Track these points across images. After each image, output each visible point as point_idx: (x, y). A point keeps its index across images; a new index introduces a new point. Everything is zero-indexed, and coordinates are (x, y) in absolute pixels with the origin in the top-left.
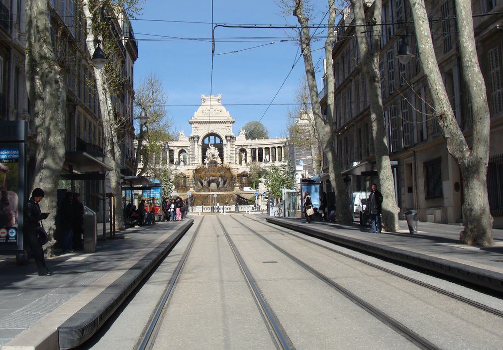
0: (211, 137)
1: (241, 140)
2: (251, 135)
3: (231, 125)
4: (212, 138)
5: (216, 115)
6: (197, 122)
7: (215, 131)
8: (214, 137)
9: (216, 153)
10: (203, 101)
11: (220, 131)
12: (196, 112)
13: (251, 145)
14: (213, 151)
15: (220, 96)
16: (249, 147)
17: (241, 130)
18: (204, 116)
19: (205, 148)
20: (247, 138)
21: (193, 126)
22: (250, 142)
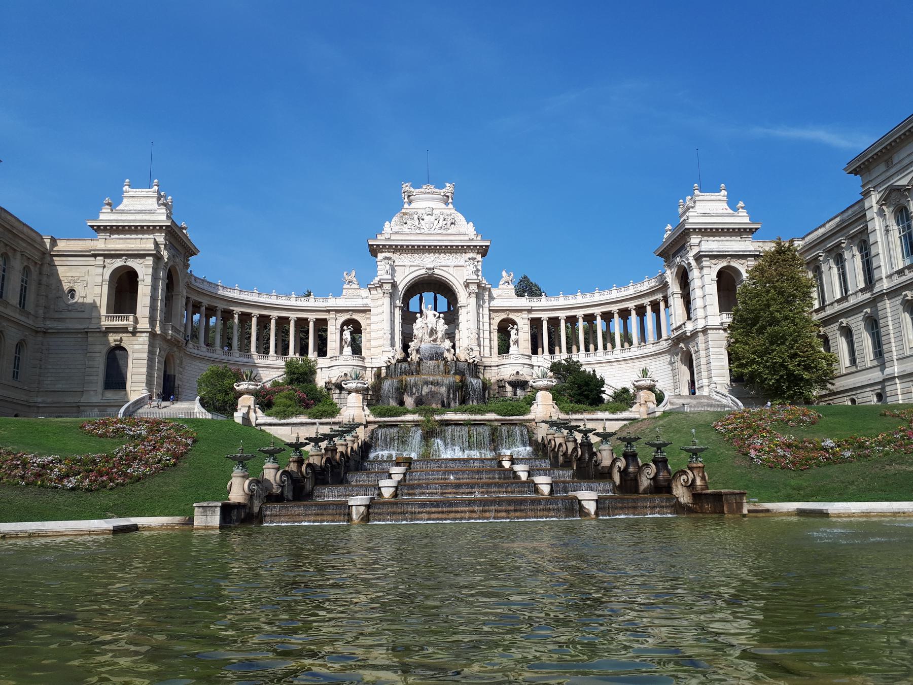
0: (424, 294)
1: (505, 296)
2: (526, 288)
3: (479, 257)
4: (428, 296)
5: (440, 232)
6: (390, 246)
7: (437, 271)
8: (432, 294)
9: (442, 327)
10: (406, 200)
11: (451, 270)
12: (387, 222)
13: (530, 311)
14: (429, 320)
15: (449, 188)
16: (525, 315)
17: (504, 274)
18: (408, 231)
19: (409, 318)
20: (519, 294)
21: (380, 256)
22: (524, 302)
